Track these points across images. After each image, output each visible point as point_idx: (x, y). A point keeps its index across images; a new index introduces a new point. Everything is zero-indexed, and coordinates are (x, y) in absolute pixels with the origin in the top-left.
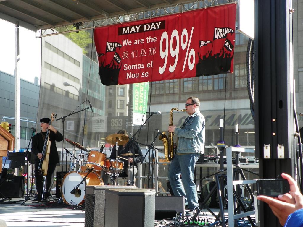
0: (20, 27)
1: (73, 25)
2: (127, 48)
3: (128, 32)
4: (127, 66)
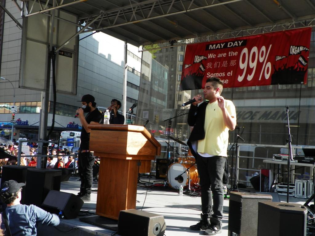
0: (128, 44)
2: (212, 60)
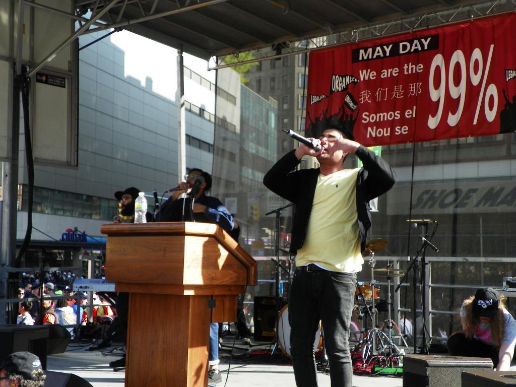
0: (185, 54)
1: (271, 47)
2: (368, 84)
3: (370, 57)
4: (369, 116)
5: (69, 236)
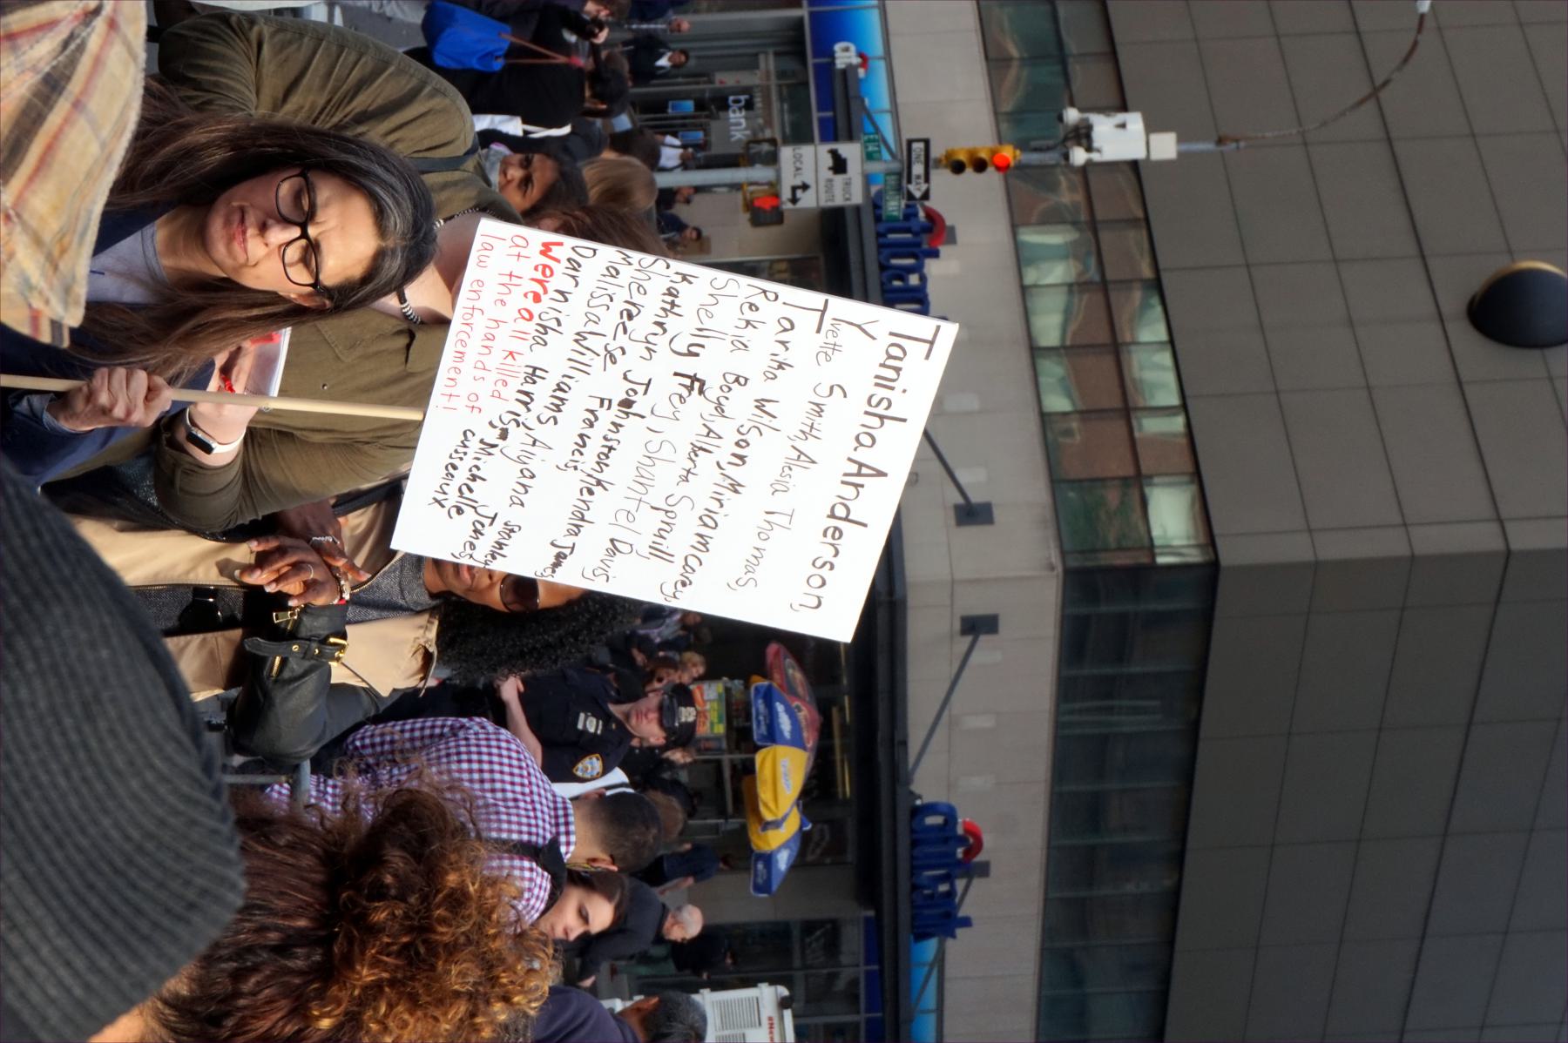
5: (946, 841)
